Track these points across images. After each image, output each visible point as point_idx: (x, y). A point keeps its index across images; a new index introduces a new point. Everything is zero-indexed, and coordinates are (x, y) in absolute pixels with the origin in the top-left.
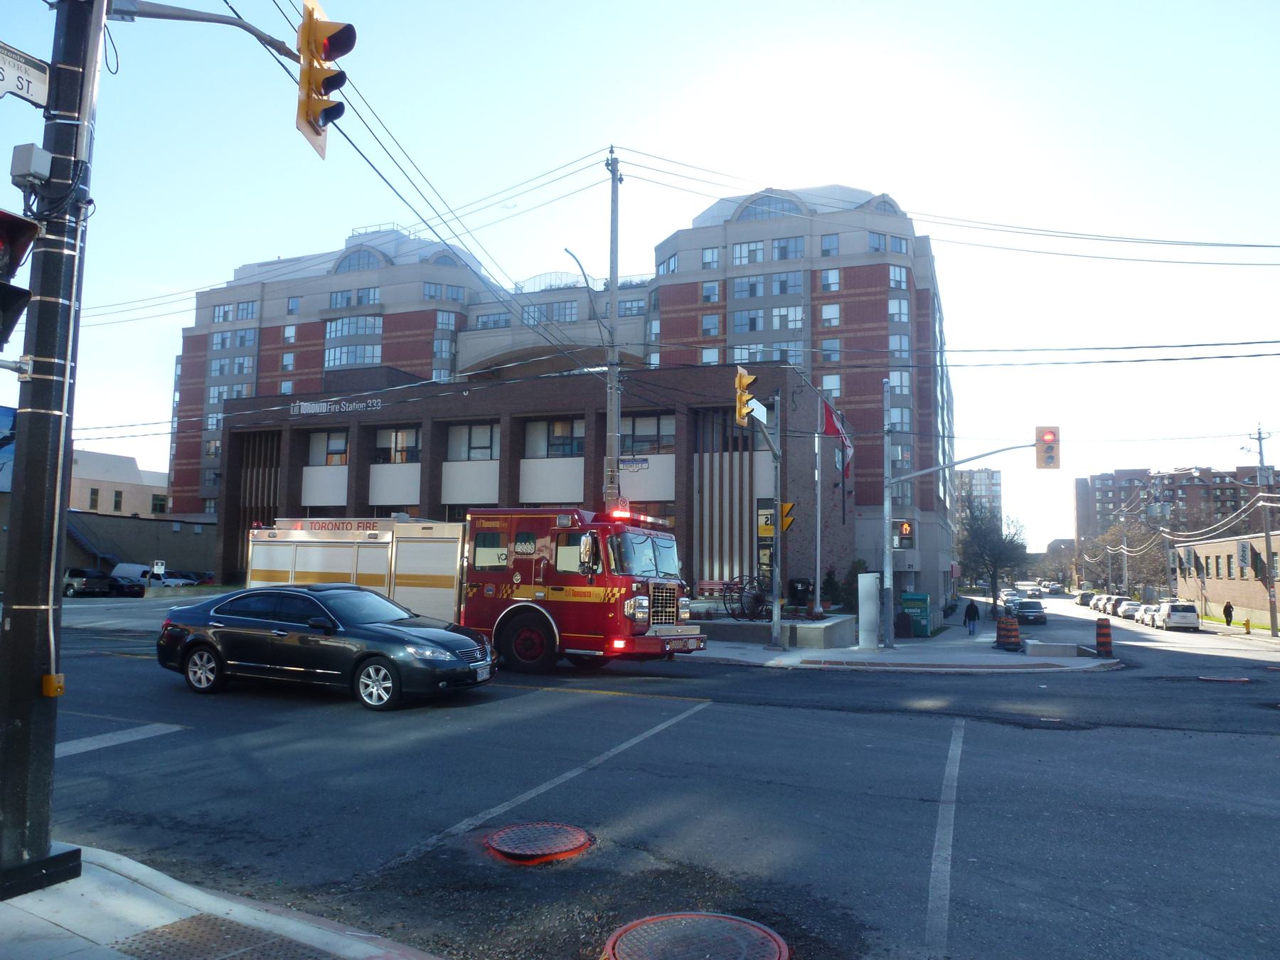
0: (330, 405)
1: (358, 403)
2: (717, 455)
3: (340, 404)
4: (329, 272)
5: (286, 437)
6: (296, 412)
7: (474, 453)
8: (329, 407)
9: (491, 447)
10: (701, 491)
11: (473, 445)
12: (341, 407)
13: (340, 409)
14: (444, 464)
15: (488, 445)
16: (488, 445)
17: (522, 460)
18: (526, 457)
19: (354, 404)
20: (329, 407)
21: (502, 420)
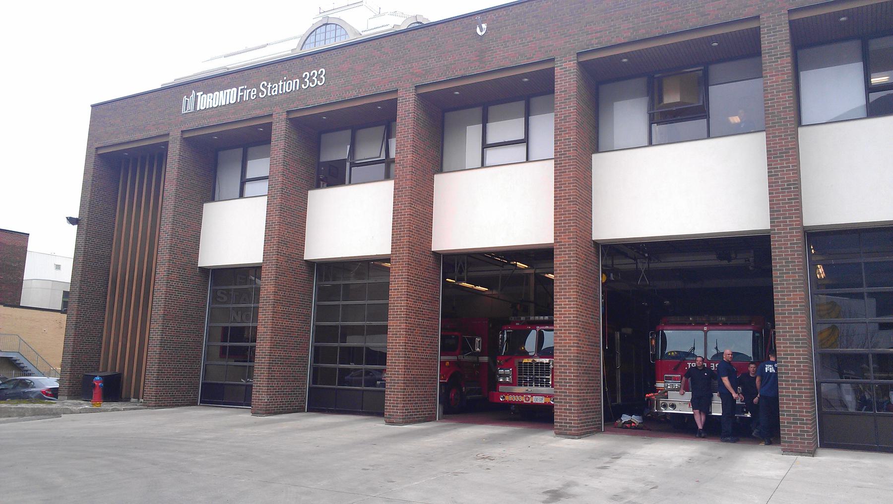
0: (242, 90)
1: (286, 81)
3: (258, 87)
5: (174, 152)
6: (191, 108)
7: (492, 155)
8: (240, 94)
9: (526, 141)
11: (490, 141)
12: (259, 91)
13: (257, 94)
14: (437, 177)
15: (522, 136)
16: (522, 136)
17: (594, 156)
19: (281, 83)
21: (558, 72)
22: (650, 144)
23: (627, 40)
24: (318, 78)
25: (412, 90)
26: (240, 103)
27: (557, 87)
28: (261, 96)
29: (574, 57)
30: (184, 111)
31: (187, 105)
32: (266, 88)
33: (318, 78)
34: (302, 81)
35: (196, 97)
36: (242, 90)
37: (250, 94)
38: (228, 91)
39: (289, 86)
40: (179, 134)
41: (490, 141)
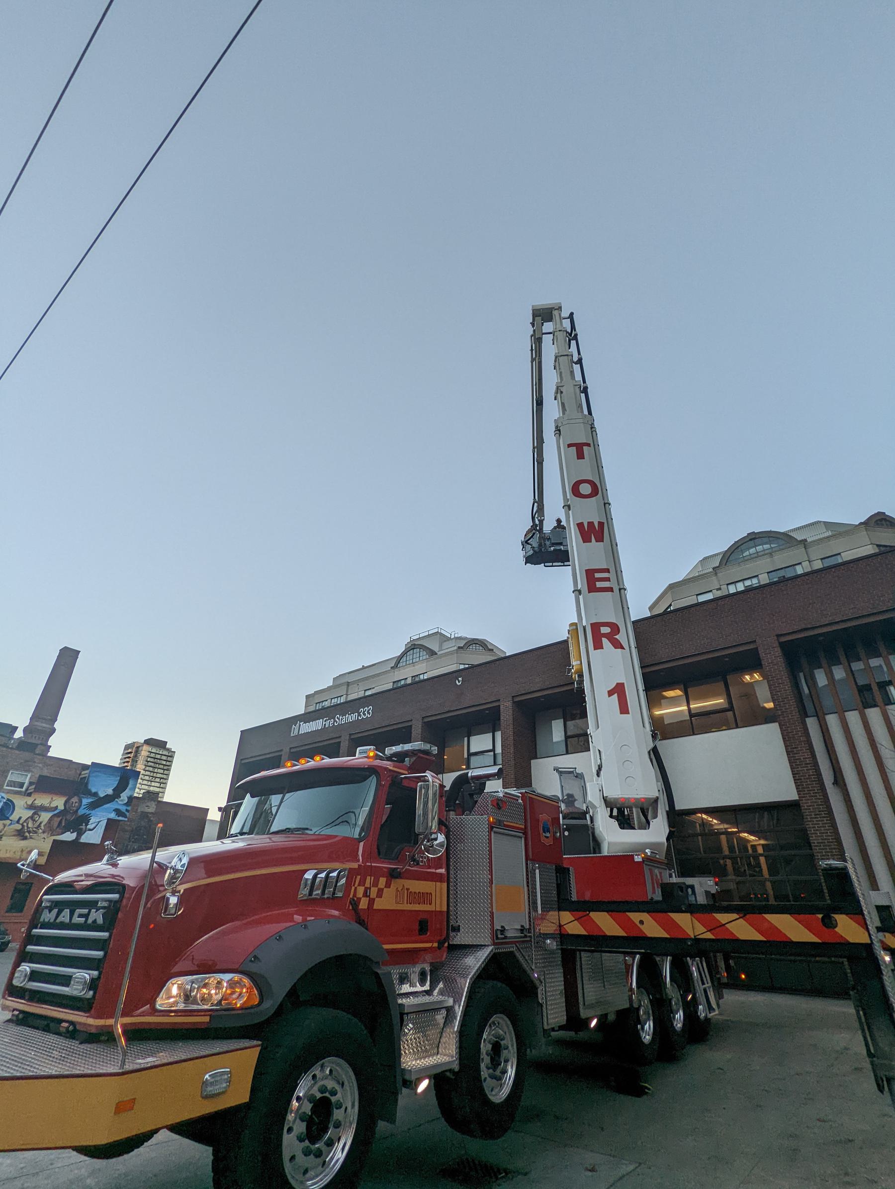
1: (350, 714)
2: (853, 717)
3: (334, 718)
4: (392, 668)
6: (296, 733)
8: (324, 723)
9: (493, 750)
10: (839, 780)
12: (335, 721)
13: (334, 723)
15: (491, 748)
16: (491, 748)
18: (538, 757)
19: (347, 716)
20: (324, 723)
21: (502, 707)
22: (567, 753)
23: (539, 689)
24: (369, 713)
25: (420, 720)
26: (324, 729)
27: (502, 718)
28: (336, 724)
29: (510, 699)
30: (292, 735)
31: (294, 731)
32: (339, 719)
33: (369, 713)
34: (359, 715)
35: (300, 725)
36: (325, 721)
37: (329, 723)
38: (318, 721)
39: (352, 718)
40: (288, 750)
41: (472, 750)
